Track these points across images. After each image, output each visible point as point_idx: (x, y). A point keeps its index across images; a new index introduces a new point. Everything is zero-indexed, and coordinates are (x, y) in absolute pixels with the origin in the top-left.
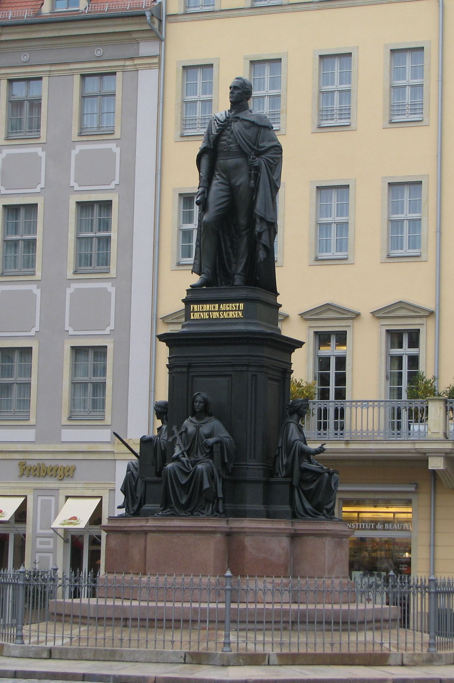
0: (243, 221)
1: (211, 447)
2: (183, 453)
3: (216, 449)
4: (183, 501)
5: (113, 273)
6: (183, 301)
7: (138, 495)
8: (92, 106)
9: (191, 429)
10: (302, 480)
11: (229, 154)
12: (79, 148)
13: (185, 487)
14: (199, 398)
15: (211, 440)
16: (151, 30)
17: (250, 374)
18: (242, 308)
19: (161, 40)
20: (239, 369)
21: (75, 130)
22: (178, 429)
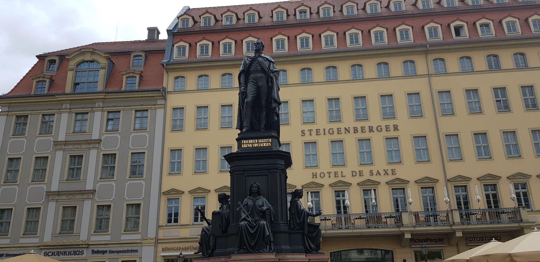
0: (264, 103)
1: (264, 212)
2: (247, 216)
3: (267, 213)
4: (252, 244)
5: (144, 177)
6: (237, 139)
7: (211, 244)
8: (138, 121)
9: (250, 203)
10: (309, 232)
11: (256, 71)
12: (133, 134)
13: (252, 236)
14: (255, 185)
15: (265, 208)
16: (163, 96)
17: (278, 174)
18: (270, 141)
19: (165, 99)
20: (272, 171)
21: (132, 129)
22: (242, 203)
